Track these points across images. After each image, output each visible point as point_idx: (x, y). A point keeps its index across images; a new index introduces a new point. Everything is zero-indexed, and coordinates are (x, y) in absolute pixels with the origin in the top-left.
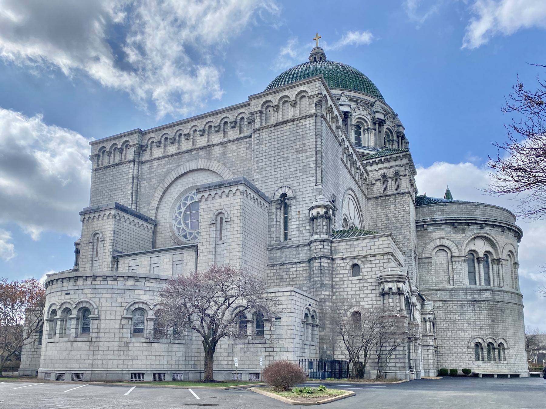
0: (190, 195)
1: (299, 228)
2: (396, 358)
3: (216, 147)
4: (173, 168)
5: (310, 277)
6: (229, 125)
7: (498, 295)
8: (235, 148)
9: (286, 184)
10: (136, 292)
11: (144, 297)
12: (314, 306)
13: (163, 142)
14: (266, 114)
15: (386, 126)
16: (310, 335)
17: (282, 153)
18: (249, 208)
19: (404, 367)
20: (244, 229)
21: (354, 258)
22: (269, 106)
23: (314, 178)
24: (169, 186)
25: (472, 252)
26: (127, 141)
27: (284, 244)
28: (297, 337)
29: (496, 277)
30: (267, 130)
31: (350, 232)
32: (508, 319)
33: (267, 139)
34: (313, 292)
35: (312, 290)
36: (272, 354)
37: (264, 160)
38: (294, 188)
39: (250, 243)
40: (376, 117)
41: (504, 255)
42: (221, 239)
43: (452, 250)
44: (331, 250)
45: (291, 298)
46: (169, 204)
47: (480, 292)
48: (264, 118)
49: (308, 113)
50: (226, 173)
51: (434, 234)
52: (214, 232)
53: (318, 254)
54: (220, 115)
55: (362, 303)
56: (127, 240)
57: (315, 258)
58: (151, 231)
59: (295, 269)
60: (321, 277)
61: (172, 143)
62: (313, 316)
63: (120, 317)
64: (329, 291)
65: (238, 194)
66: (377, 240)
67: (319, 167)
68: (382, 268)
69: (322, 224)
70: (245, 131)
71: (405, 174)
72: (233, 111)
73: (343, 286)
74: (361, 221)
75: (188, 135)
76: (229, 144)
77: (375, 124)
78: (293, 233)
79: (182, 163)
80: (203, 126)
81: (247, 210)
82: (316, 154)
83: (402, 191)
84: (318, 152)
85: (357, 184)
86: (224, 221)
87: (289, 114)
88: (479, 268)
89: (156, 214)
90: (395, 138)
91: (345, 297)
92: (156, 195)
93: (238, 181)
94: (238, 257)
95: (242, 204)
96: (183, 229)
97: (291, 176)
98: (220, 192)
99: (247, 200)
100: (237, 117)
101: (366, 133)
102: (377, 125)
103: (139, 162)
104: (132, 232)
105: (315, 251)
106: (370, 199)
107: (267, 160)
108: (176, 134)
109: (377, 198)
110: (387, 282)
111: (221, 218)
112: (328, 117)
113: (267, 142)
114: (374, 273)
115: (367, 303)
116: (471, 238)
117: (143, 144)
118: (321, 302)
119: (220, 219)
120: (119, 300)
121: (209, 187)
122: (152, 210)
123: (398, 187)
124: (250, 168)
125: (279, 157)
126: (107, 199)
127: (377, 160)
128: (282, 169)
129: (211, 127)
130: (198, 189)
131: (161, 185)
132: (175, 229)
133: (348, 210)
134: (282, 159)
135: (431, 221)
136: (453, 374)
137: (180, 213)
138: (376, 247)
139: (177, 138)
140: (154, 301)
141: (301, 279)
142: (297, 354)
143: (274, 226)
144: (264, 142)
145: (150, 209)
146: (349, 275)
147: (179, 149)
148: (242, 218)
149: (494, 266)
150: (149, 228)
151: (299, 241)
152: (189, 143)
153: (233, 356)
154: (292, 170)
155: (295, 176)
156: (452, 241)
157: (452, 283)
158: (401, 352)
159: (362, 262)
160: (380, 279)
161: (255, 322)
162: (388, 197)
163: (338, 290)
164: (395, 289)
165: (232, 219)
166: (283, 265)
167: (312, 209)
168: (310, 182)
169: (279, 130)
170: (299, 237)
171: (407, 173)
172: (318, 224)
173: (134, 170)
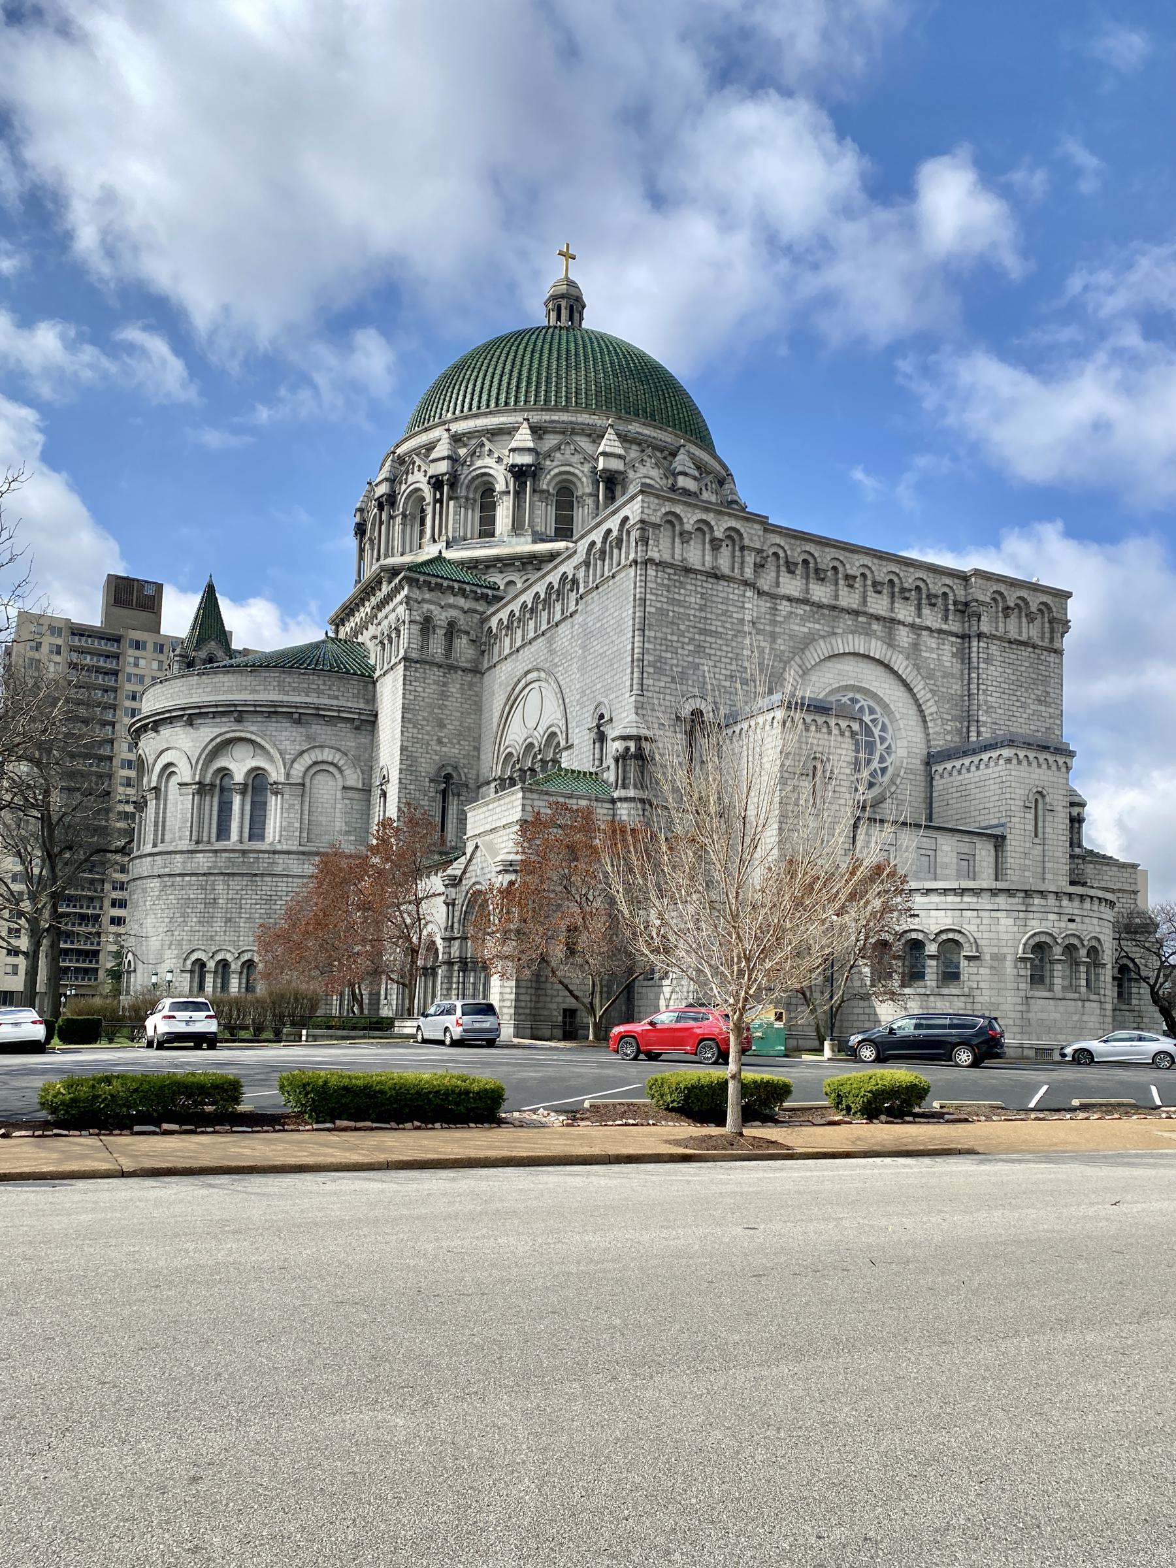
3: (901, 627)
4: (822, 633)
8: (934, 646)
30: (998, 642)
76: (924, 633)
126: (691, 648)
152: (852, 595)
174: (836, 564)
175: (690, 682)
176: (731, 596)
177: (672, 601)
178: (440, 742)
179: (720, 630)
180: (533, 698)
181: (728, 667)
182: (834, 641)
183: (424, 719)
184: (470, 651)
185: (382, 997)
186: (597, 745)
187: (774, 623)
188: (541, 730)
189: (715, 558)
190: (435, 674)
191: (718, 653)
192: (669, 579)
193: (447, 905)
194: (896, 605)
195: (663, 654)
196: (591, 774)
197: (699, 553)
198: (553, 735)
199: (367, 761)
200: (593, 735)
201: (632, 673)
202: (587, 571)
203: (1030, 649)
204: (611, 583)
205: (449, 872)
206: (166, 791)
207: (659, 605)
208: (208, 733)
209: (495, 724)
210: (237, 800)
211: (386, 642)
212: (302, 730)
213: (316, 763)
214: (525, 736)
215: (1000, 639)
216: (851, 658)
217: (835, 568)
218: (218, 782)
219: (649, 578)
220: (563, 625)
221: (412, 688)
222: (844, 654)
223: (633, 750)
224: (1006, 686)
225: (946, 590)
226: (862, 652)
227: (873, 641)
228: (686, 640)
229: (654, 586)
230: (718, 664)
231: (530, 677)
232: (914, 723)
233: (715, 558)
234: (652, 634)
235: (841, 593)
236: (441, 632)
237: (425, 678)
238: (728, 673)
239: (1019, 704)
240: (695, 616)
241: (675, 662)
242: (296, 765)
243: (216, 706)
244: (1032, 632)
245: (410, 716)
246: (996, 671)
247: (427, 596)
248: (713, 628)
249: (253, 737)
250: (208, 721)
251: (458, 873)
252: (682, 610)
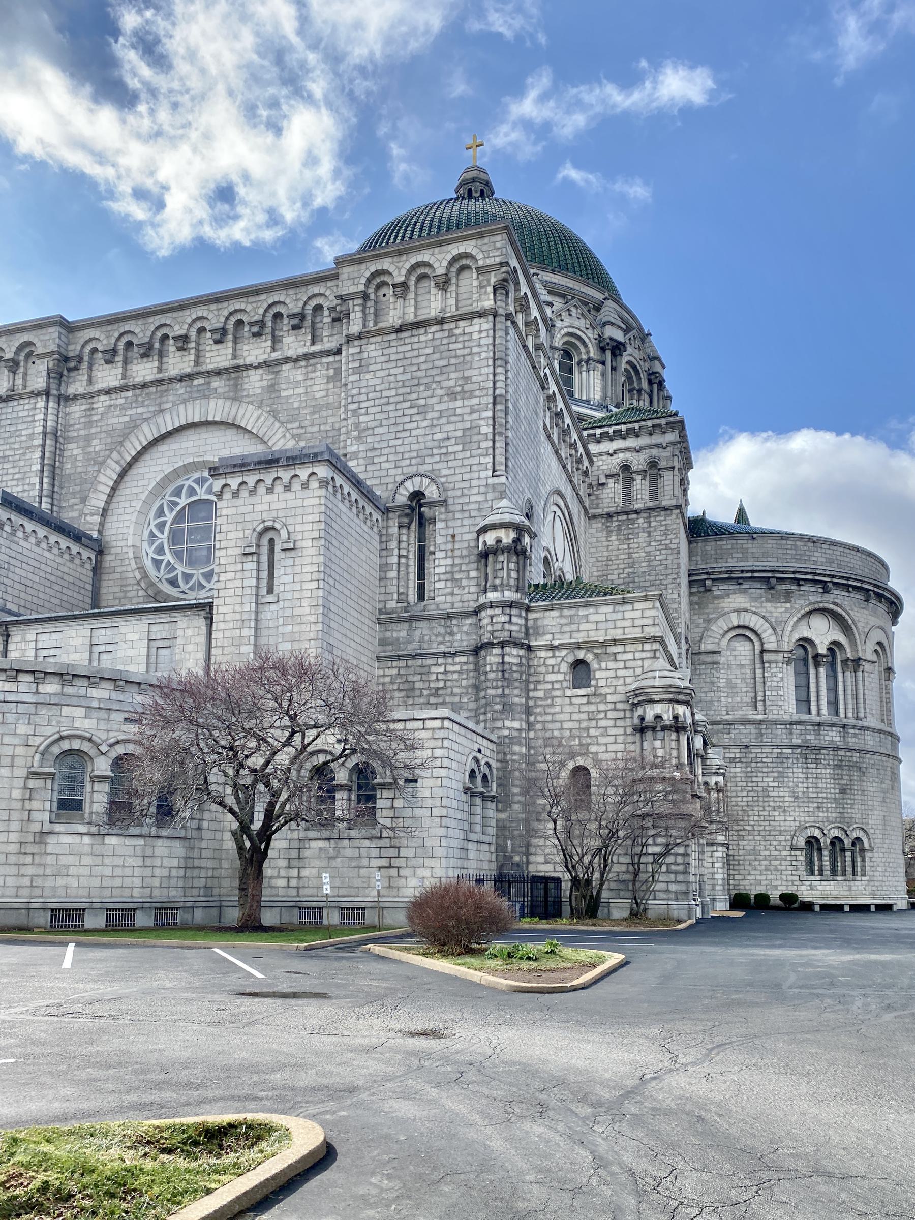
0: (187, 483)
1: (452, 573)
2: (668, 872)
3: (252, 372)
4: (145, 416)
5: (477, 688)
6: (286, 321)
7: (855, 735)
8: (300, 378)
9: (423, 469)
10: (66, 710)
11: (85, 724)
12: (488, 753)
13: (121, 352)
14: (376, 303)
15: (625, 358)
16: (478, 819)
17: (414, 396)
18: (338, 520)
19: (686, 893)
20: (328, 571)
21: (578, 646)
22: (384, 284)
23: (489, 459)
24: (136, 459)
25: (805, 643)
26: (30, 344)
27: (417, 610)
28: (454, 824)
29: (850, 697)
30: (379, 339)
31: (558, 590)
32: (872, 786)
33: (379, 360)
34: (485, 721)
35: (482, 717)
36: (395, 862)
37: (371, 410)
38: (443, 480)
39: (339, 603)
40: (607, 335)
41: (867, 651)
42: (270, 591)
43: (763, 636)
44: (527, 629)
45: (441, 734)
46: (134, 504)
47: (819, 730)
48: (372, 310)
49: (477, 307)
50: (278, 436)
51: (727, 600)
52: (254, 572)
53: (496, 634)
54: (263, 297)
55: (593, 749)
56: (30, 584)
57: (490, 645)
58: (88, 566)
59: (442, 669)
60: (503, 687)
61: (145, 355)
62: (485, 776)
63: (23, 772)
64: (521, 720)
65: (314, 484)
66: (629, 607)
67: (501, 434)
68: (639, 671)
69: (506, 566)
70: (325, 339)
71: (670, 465)
72: (298, 290)
73: (552, 710)
74: (577, 567)
75: (185, 338)
76: (284, 367)
77: (603, 349)
78: (437, 584)
79: (169, 405)
80: (223, 320)
81: (334, 525)
82: (494, 404)
83: (664, 503)
84: (498, 399)
85: (571, 481)
86: (277, 548)
87: (433, 305)
88: (817, 678)
89: (102, 524)
90: (645, 385)
91: (556, 733)
92: (102, 478)
93: (316, 455)
94: (312, 635)
95: (323, 509)
96: (169, 563)
97: (435, 451)
98: (268, 478)
99: (335, 502)
100: (305, 303)
101: (584, 368)
102: (608, 353)
103: (59, 397)
104: (43, 566)
105: (490, 628)
106: (595, 517)
107: (379, 409)
108: (153, 333)
109: (609, 516)
110: (652, 701)
111: (271, 541)
112: (520, 319)
113: (379, 366)
114: (621, 681)
115: (603, 748)
116: (803, 612)
117: (71, 354)
118: (503, 745)
119: (267, 544)
120: (22, 729)
121: (243, 465)
122: (91, 514)
123: (654, 494)
124: (337, 426)
125: (408, 404)
127: (611, 430)
128: (414, 433)
129: (240, 323)
130: (215, 468)
131: (115, 455)
132: (148, 564)
133: (550, 538)
134: (415, 411)
135: (720, 573)
136: (762, 902)
137: (161, 526)
138: (627, 623)
139: (157, 345)
140: (111, 734)
141: (456, 690)
142: (453, 862)
143: (395, 567)
144: (372, 368)
145: (87, 512)
146: (565, 684)
147: (160, 370)
148: (322, 542)
149: (848, 674)
150: (85, 557)
151: (453, 604)
152: (186, 359)
153: (310, 867)
154: (438, 436)
155: (444, 451)
156: (763, 617)
157: (760, 708)
158: (680, 859)
159: (596, 655)
160: (637, 696)
161: (355, 787)
162: (634, 516)
163: (539, 719)
164: (667, 717)
165: (299, 544)
166: (414, 657)
167: (484, 530)
168: (480, 467)
169: (407, 341)
170: (452, 594)
171: (676, 464)
172: (499, 566)
173: (46, 414)
176: (21, 414)
203: (434, 329)
216: (191, 431)
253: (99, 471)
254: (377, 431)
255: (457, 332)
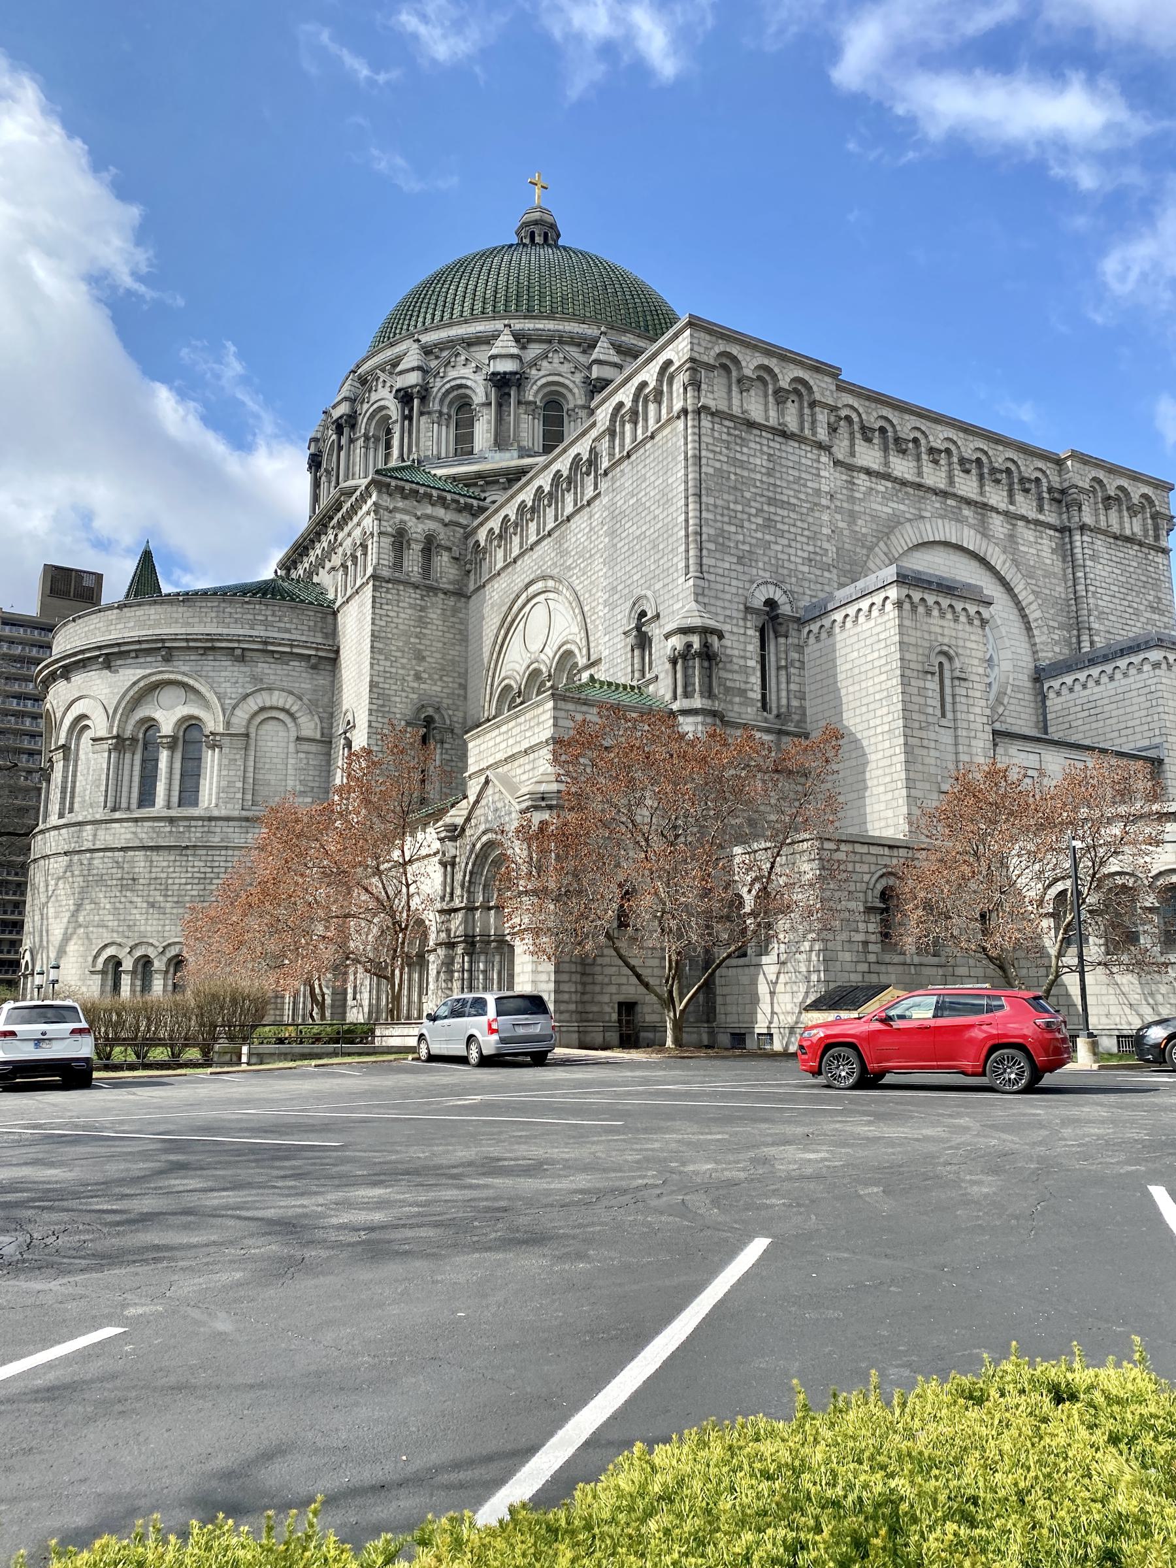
3: (994, 515)
4: (908, 516)
8: (1032, 539)
76: (1020, 523)
131: (881, 544)
152: (938, 473)
174: (918, 435)
175: (760, 565)
176: (803, 460)
177: (733, 461)
178: (418, 677)
179: (793, 501)
180: (538, 616)
181: (805, 547)
182: (922, 526)
183: (399, 650)
184: (457, 572)
185: (350, 996)
186: (636, 652)
187: (851, 499)
188: (549, 651)
189: (781, 413)
190: (410, 597)
191: (793, 529)
192: (729, 434)
193: (444, 864)
194: (987, 488)
195: (726, 527)
196: (632, 688)
197: (761, 407)
198: (569, 654)
199: (327, 705)
200: (631, 640)
201: (687, 551)
202: (612, 440)
203: (1136, 547)
204: (648, 446)
205: (447, 819)
206: (77, 750)
207: (718, 465)
208: (129, 675)
209: (486, 655)
210: (164, 755)
211: (349, 563)
212: (243, 669)
213: (263, 709)
214: (528, 661)
215: (1105, 533)
216: (941, 549)
217: (916, 441)
218: (141, 736)
219: (703, 431)
220: (577, 517)
221: (383, 612)
222: (934, 542)
223: (696, 646)
224: (1116, 589)
225: (1040, 475)
226: (954, 541)
227: (966, 529)
228: (753, 511)
229: (710, 440)
230: (793, 544)
231: (532, 589)
232: (1016, 631)
233: (781, 413)
234: (711, 500)
235: (925, 469)
236: (417, 547)
237: (398, 601)
238: (806, 555)
239: (1131, 611)
240: (761, 481)
241: (741, 538)
242: (238, 712)
243: (139, 642)
244: (1134, 526)
245: (380, 646)
246: (1104, 567)
247: (400, 504)
248: (785, 498)
249: (185, 679)
250: (130, 661)
251: (460, 821)
252: (746, 474)
253: (868, 556)
254: (1111, 617)
255: (1150, 557)
